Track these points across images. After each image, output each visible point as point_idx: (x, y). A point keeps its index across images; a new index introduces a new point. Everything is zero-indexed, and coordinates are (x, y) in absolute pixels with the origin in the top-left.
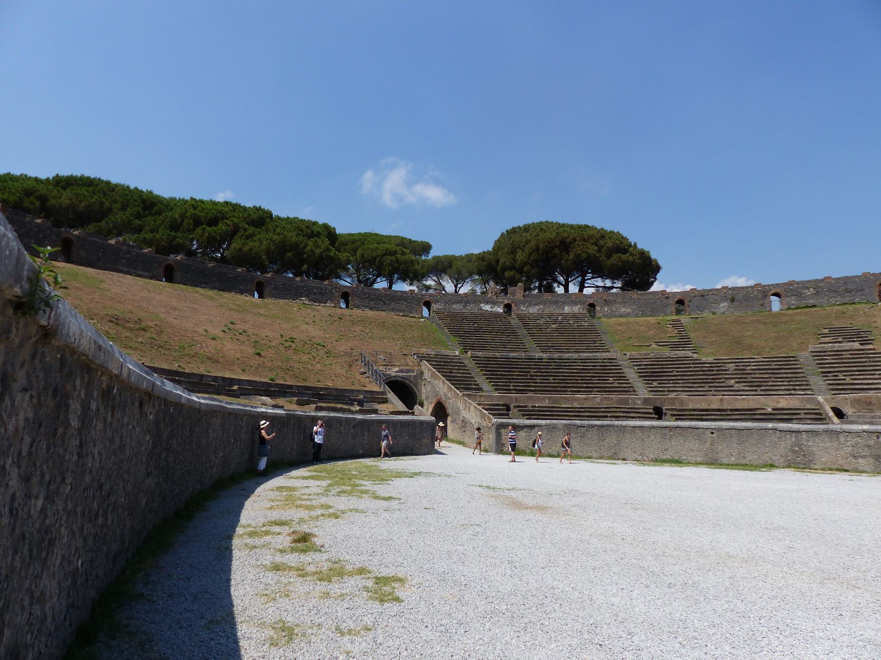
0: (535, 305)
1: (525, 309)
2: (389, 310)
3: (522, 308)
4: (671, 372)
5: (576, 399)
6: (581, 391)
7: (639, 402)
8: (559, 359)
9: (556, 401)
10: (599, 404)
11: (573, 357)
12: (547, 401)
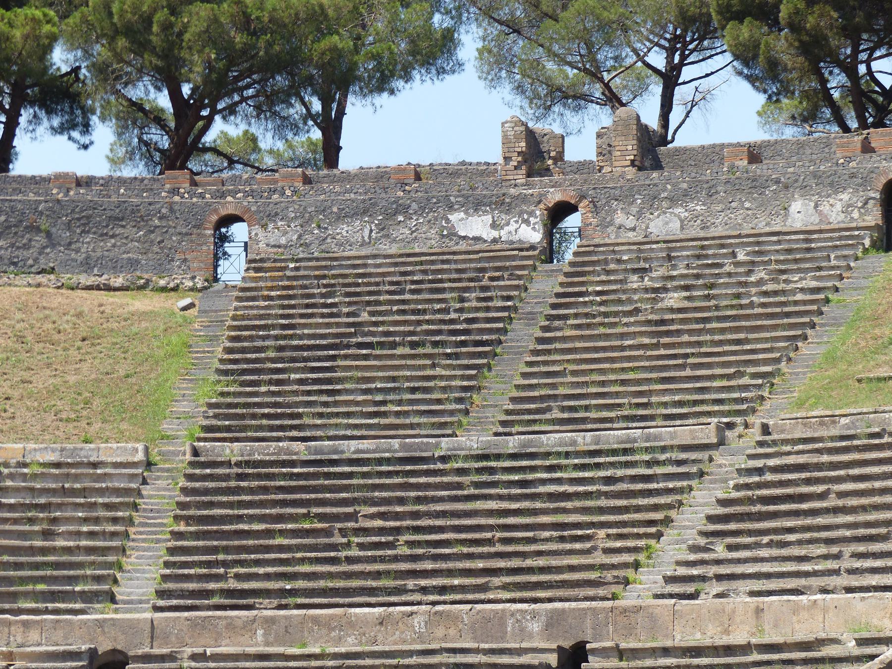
0: (673, 201)
1: (630, 222)
2: (68, 265)
3: (620, 218)
4: (823, 496)
5: (351, 625)
6: (453, 589)
7: (535, 627)
8: (567, 455)
9: (288, 633)
10: (420, 638)
11: (574, 443)
12: (260, 632)
